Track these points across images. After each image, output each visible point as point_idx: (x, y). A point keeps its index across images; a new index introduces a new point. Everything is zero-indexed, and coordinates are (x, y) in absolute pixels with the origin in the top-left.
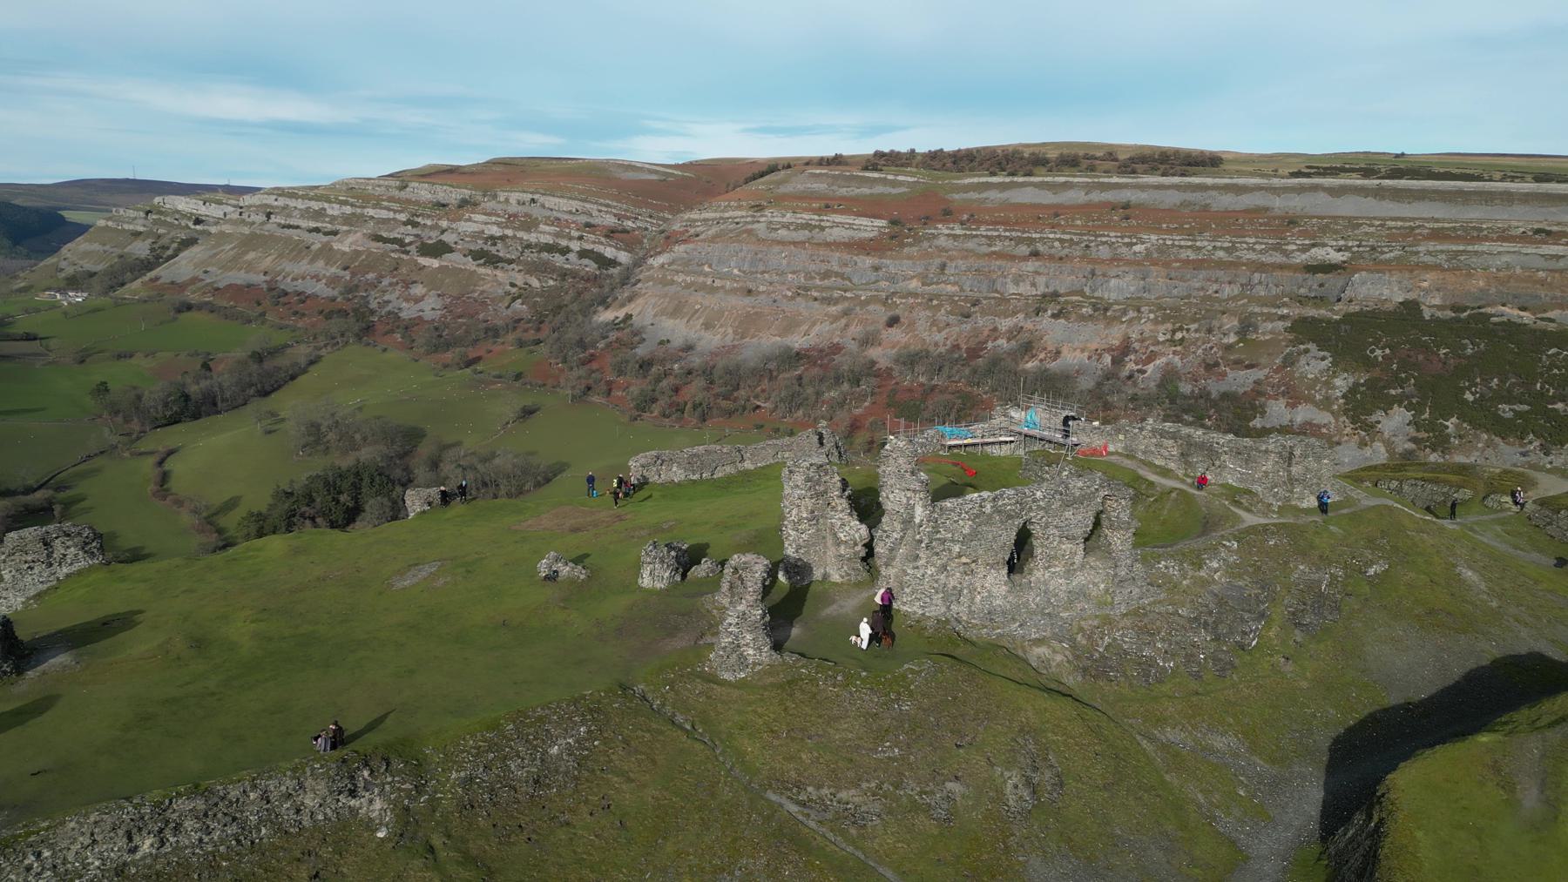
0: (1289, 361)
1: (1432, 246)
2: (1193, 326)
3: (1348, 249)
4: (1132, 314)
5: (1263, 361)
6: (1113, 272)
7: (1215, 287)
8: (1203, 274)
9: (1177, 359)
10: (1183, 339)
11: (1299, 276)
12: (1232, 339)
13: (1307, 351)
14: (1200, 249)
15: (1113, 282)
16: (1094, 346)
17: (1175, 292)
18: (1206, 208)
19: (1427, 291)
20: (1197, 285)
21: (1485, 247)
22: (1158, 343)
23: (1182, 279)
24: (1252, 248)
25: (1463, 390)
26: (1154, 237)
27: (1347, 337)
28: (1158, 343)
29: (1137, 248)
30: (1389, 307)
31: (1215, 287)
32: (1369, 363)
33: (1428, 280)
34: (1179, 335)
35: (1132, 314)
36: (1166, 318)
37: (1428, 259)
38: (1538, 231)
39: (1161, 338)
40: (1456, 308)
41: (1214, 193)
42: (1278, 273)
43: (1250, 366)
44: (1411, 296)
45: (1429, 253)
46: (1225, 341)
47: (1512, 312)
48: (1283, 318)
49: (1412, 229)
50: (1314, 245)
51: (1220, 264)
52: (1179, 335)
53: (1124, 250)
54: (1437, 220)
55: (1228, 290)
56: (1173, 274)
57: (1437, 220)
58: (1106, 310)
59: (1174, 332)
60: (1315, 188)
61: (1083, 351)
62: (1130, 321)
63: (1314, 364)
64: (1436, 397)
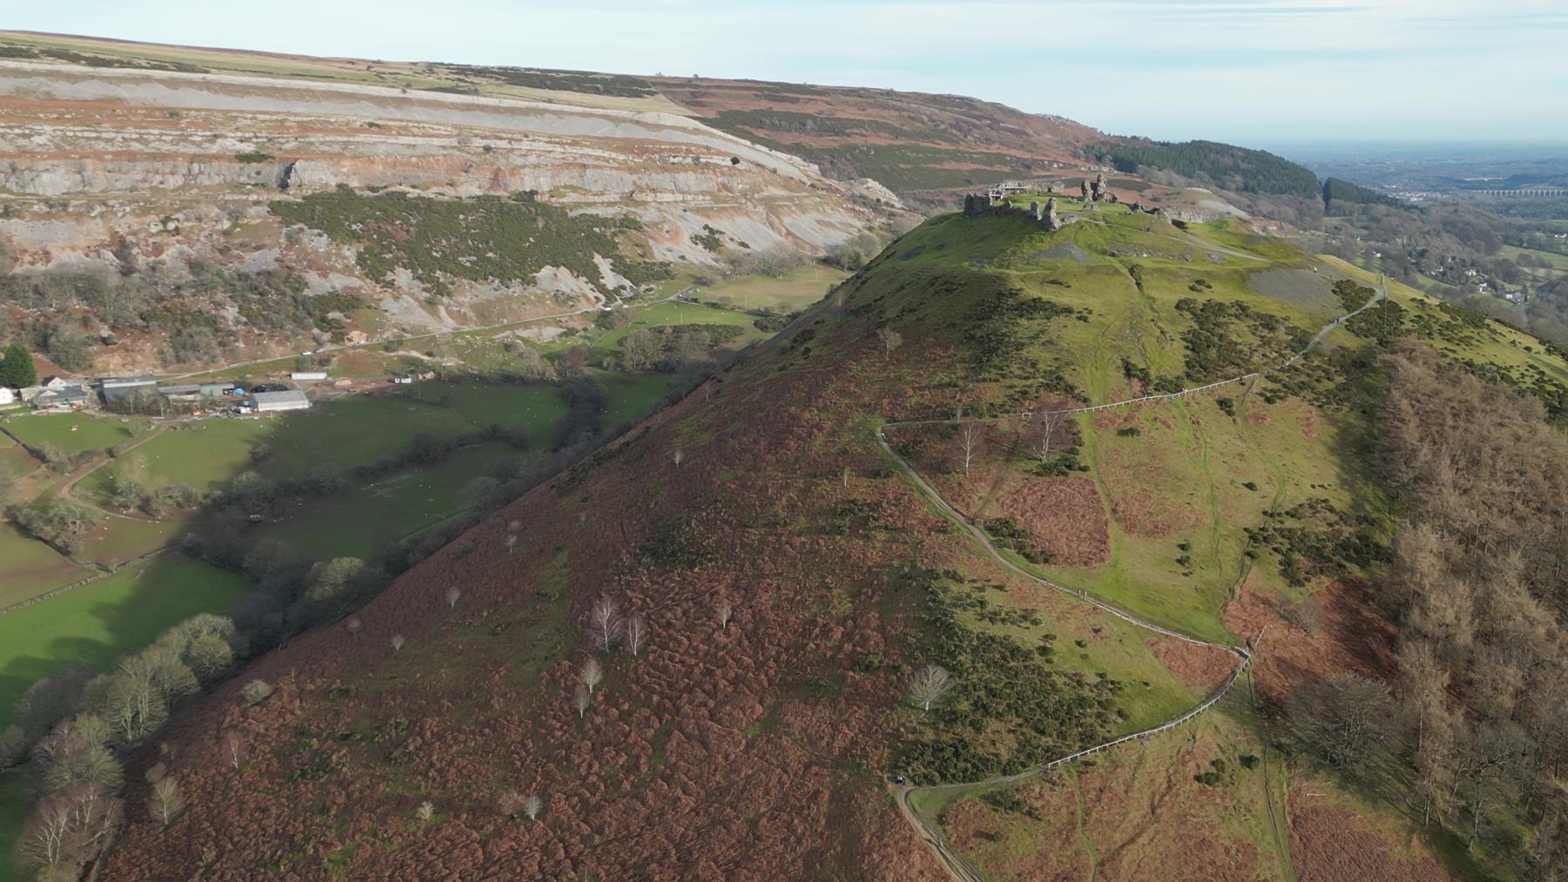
0: (292, 240)
1: (320, 137)
2: (180, 216)
3: (248, 140)
4: (99, 209)
5: (268, 241)
6: (41, 165)
7: (159, 178)
8: (140, 166)
9: (185, 248)
10: (177, 229)
11: (237, 166)
12: (226, 225)
13: (301, 230)
14: (108, 141)
15: (45, 176)
16: (84, 244)
17: (118, 185)
18: (50, 97)
19: (347, 175)
20: (139, 177)
21: (361, 138)
22: (153, 235)
23: (120, 171)
24: (161, 139)
25: (429, 252)
26: (48, 128)
27: (331, 211)
28: (153, 235)
29: (37, 139)
30: (332, 189)
31: (159, 178)
32: (356, 237)
33: (346, 166)
34: (171, 226)
35: (99, 209)
36: (145, 212)
37: (326, 149)
38: (371, 125)
39: (154, 230)
40: (373, 189)
41: (43, 80)
42: (215, 164)
43: (257, 248)
44: (339, 180)
45: (322, 143)
46: (219, 227)
47: (413, 193)
48: (256, 203)
49: (282, 122)
50: (216, 136)
51: (164, 157)
52: (171, 226)
53: (22, 142)
54: (295, 115)
55: (174, 182)
56: (110, 167)
57: (295, 115)
58: (65, 206)
59: (164, 222)
60: (147, 79)
61: (73, 249)
62: (102, 215)
63: (318, 242)
64: (416, 260)
